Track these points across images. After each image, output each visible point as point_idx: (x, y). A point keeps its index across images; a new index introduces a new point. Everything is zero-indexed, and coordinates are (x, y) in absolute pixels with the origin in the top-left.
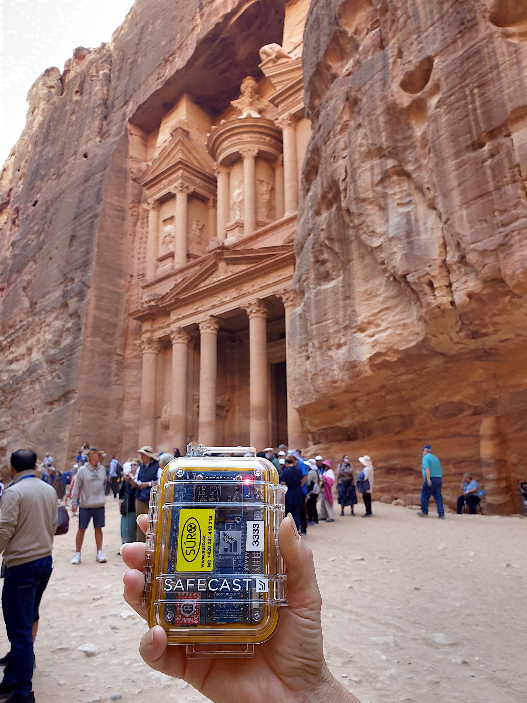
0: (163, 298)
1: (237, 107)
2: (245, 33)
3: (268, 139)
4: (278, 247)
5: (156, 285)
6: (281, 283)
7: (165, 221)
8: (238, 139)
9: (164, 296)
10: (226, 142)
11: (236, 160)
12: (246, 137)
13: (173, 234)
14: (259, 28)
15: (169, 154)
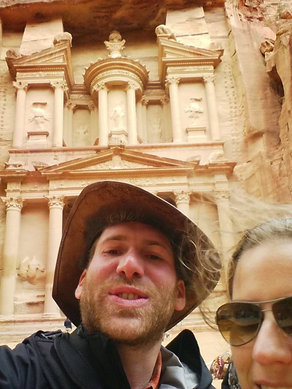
0: (49, 168)
1: (108, 47)
2: (132, 5)
3: (141, 82)
4: (181, 161)
5: (29, 154)
6: (176, 185)
7: (35, 104)
8: (126, 73)
9: (50, 167)
10: (116, 71)
11: (121, 86)
12: (131, 74)
13: (46, 117)
14: (141, 8)
15: (52, 54)
